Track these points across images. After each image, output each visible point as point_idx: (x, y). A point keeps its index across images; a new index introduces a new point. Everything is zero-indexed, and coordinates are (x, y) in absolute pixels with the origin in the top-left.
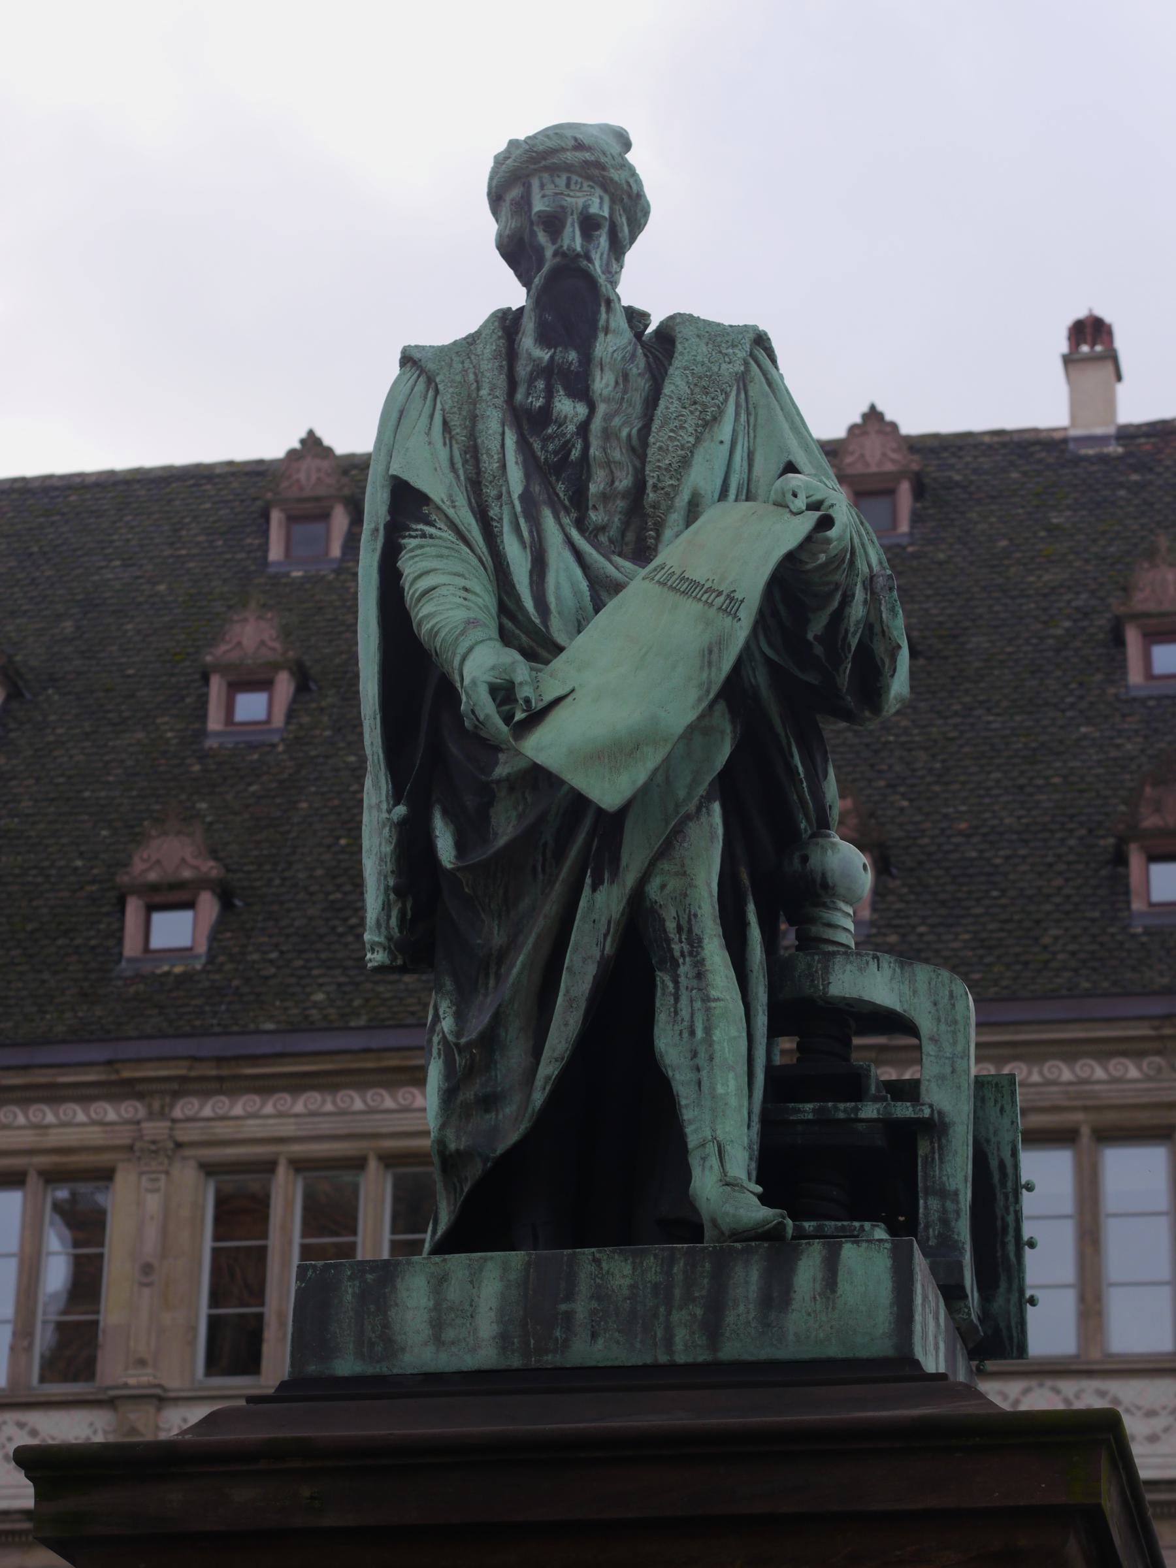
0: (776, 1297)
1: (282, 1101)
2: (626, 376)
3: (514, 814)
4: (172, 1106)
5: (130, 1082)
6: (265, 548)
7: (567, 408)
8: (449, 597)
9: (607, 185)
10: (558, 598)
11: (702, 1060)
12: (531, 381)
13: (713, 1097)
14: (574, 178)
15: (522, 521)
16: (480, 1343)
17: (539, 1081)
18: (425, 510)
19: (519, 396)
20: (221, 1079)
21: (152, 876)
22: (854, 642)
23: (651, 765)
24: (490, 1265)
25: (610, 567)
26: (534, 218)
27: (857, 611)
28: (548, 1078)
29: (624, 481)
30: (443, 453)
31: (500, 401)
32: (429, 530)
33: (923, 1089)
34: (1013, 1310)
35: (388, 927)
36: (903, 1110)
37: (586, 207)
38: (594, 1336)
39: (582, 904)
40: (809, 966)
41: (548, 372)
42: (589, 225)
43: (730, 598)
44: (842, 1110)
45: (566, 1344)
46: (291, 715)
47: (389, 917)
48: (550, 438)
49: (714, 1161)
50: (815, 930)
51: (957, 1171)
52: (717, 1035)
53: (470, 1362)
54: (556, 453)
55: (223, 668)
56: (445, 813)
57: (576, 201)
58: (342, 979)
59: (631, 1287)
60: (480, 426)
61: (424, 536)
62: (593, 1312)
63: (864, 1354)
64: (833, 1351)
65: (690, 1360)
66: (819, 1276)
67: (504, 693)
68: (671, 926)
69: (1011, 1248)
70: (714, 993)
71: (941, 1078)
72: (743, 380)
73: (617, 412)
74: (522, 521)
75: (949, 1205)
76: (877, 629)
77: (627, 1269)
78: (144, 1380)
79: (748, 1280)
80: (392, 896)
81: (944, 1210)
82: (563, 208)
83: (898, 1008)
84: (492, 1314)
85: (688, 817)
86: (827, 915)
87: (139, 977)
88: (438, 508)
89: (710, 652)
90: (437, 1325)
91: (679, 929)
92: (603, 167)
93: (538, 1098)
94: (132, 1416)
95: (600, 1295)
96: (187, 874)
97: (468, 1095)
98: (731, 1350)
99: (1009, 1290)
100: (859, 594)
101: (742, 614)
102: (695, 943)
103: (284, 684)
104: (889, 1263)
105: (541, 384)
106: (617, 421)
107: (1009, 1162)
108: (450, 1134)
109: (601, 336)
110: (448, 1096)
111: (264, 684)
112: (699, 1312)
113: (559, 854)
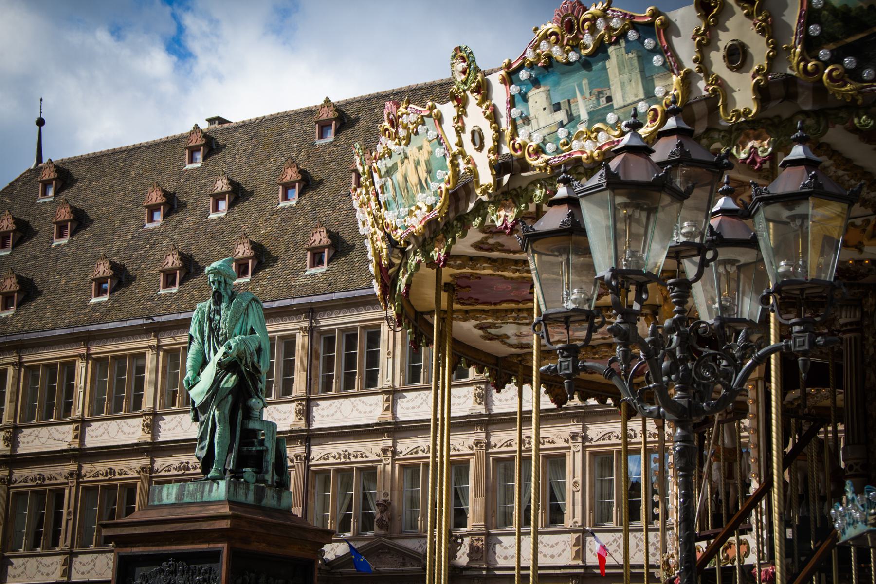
0: (210, 491)
7: (217, 317)
16: (172, 499)
27: (249, 360)
36: (259, 448)
98: (205, 499)
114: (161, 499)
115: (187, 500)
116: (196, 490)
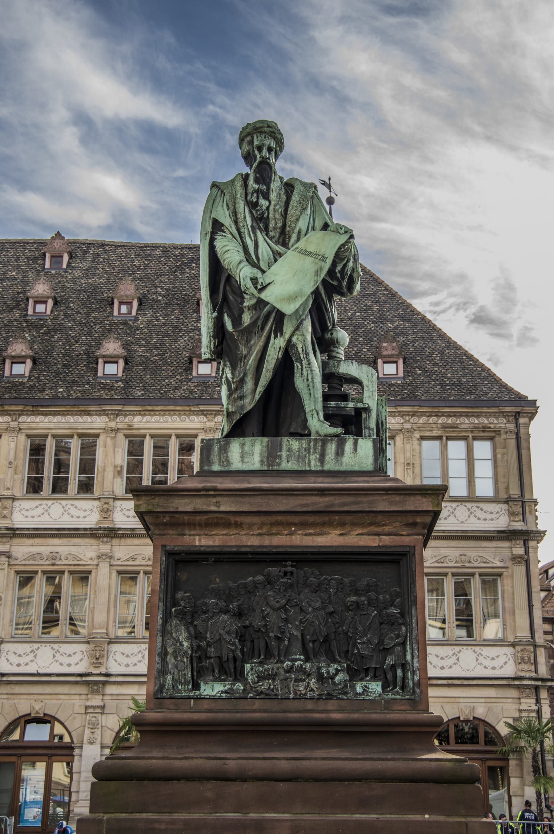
0: (340, 453)
1: (50, 418)
2: (280, 194)
3: (249, 317)
4: (19, 418)
5: (7, 411)
6: (44, 264)
7: (263, 202)
8: (230, 253)
9: (275, 138)
10: (262, 256)
11: (311, 387)
12: (252, 194)
13: (315, 398)
14: (267, 135)
15: (251, 233)
16: (255, 462)
17: (257, 392)
18: (222, 228)
19: (249, 198)
20: (33, 411)
21: (13, 354)
22: (349, 273)
23: (300, 303)
24: (257, 441)
25: (279, 249)
26: (254, 146)
27: (351, 264)
28: (260, 392)
29: (280, 224)
30: (227, 213)
31: (244, 199)
32: (224, 234)
33: (364, 400)
34: (384, 462)
35: (210, 347)
36: (360, 405)
37: (270, 144)
38: (288, 462)
39: (271, 343)
40: (334, 364)
41: (257, 191)
42: (270, 149)
43: (323, 256)
44: (343, 404)
45: (280, 464)
46: (52, 311)
47: (210, 345)
48: (258, 210)
49: (316, 415)
50: (334, 354)
51: (373, 423)
52: (315, 380)
53: (252, 468)
54: (260, 215)
55: (33, 298)
56: (228, 315)
57: (267, 142)
58: (67, 385)
59: (299, 448)
60: (237, 206)
61: (223, 236)
62: (288, 455)
63: (365, 469)
64: (356, 468)
65: (316, 470)
66: (352, 447)
67: (254, 280)
68: (300, 350)
69: (384, 445)
70: (313, 369)
71: (369, 397)
72: (312, 198)
73: (278, 204)
74: (251, 233)
75: (371, 431)
76: (356, 270)
77: (297, 443)
78: (9, 494)
79: (332, 448)
80: (212, 339)
81: (370, 433)
82: (263, 144)
83: (358, 377)
84: (258, 455)
85: (303, 320)
86: (338, 350)
87: (8, 382)
88: (227, 228)
89: (317, 272)
90: (242, 457)
91: (303, 350)
92: (275, 133)
93: (257, 397)
94: (6, 503)
95: (289, 450)
96: (23, 354)
97: (235, 396)
98: (327, 467)
99: (383, 456)
100: (352, 260)
101: (327, 261)
102: (307, 355)
103: (50, 303)
104: (372, 444)
105: (255, 195)
106: (278, 207)
107: (384, 421)
108: (230, 406)
109: (272, 182)
110: (229, 396)
111: (45, 303)
112: (318, 456)
113: (263, 329)
114: (228, 462)
115: (285, 466)
116: (308, 450)
